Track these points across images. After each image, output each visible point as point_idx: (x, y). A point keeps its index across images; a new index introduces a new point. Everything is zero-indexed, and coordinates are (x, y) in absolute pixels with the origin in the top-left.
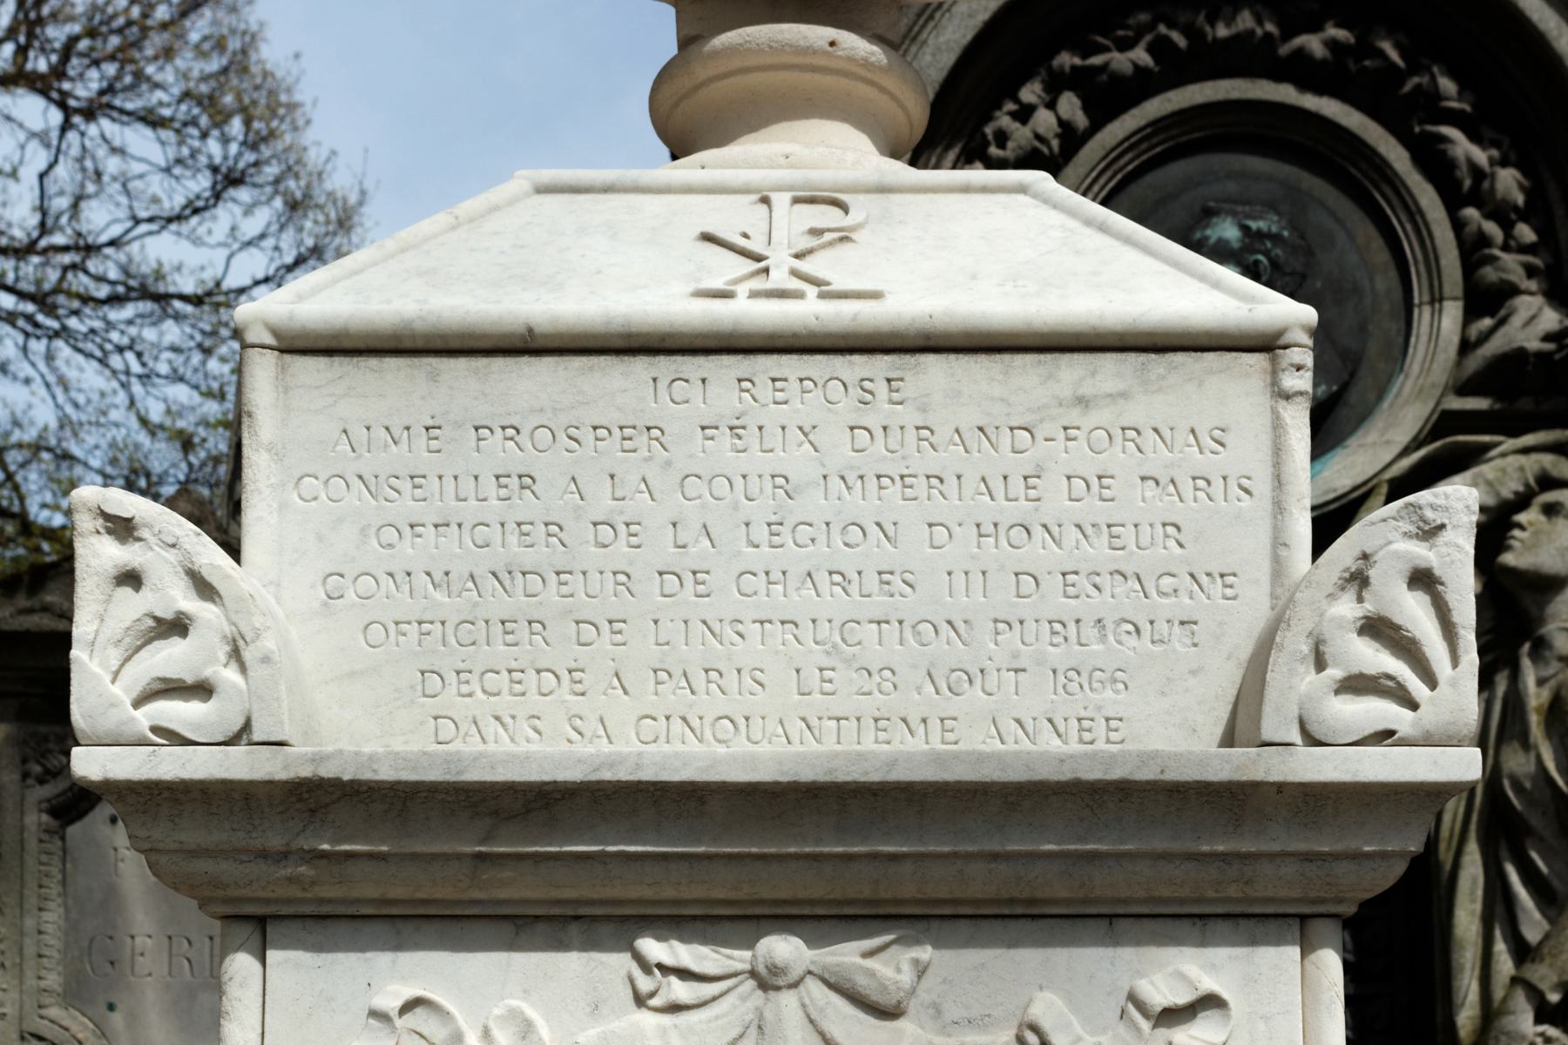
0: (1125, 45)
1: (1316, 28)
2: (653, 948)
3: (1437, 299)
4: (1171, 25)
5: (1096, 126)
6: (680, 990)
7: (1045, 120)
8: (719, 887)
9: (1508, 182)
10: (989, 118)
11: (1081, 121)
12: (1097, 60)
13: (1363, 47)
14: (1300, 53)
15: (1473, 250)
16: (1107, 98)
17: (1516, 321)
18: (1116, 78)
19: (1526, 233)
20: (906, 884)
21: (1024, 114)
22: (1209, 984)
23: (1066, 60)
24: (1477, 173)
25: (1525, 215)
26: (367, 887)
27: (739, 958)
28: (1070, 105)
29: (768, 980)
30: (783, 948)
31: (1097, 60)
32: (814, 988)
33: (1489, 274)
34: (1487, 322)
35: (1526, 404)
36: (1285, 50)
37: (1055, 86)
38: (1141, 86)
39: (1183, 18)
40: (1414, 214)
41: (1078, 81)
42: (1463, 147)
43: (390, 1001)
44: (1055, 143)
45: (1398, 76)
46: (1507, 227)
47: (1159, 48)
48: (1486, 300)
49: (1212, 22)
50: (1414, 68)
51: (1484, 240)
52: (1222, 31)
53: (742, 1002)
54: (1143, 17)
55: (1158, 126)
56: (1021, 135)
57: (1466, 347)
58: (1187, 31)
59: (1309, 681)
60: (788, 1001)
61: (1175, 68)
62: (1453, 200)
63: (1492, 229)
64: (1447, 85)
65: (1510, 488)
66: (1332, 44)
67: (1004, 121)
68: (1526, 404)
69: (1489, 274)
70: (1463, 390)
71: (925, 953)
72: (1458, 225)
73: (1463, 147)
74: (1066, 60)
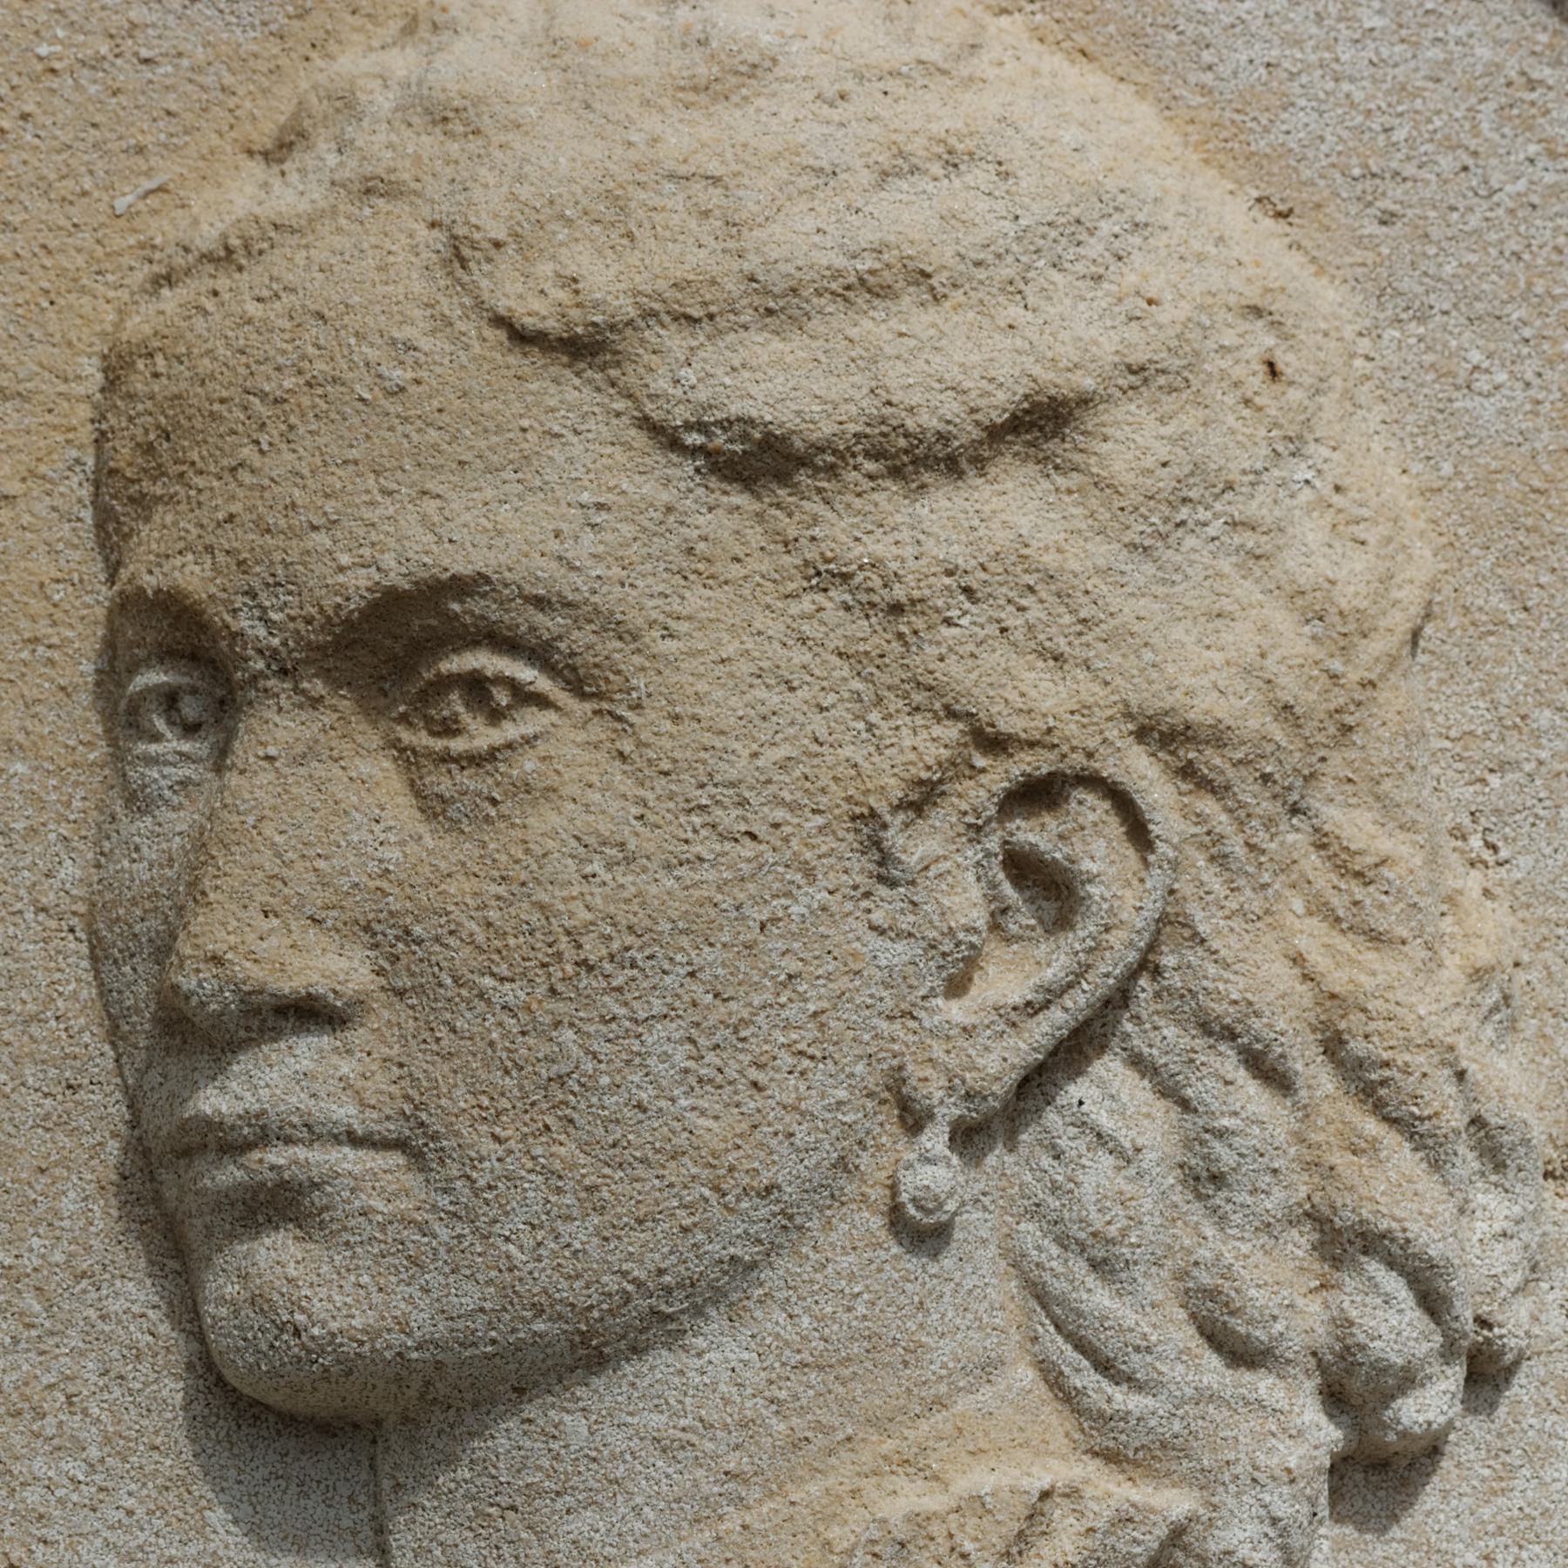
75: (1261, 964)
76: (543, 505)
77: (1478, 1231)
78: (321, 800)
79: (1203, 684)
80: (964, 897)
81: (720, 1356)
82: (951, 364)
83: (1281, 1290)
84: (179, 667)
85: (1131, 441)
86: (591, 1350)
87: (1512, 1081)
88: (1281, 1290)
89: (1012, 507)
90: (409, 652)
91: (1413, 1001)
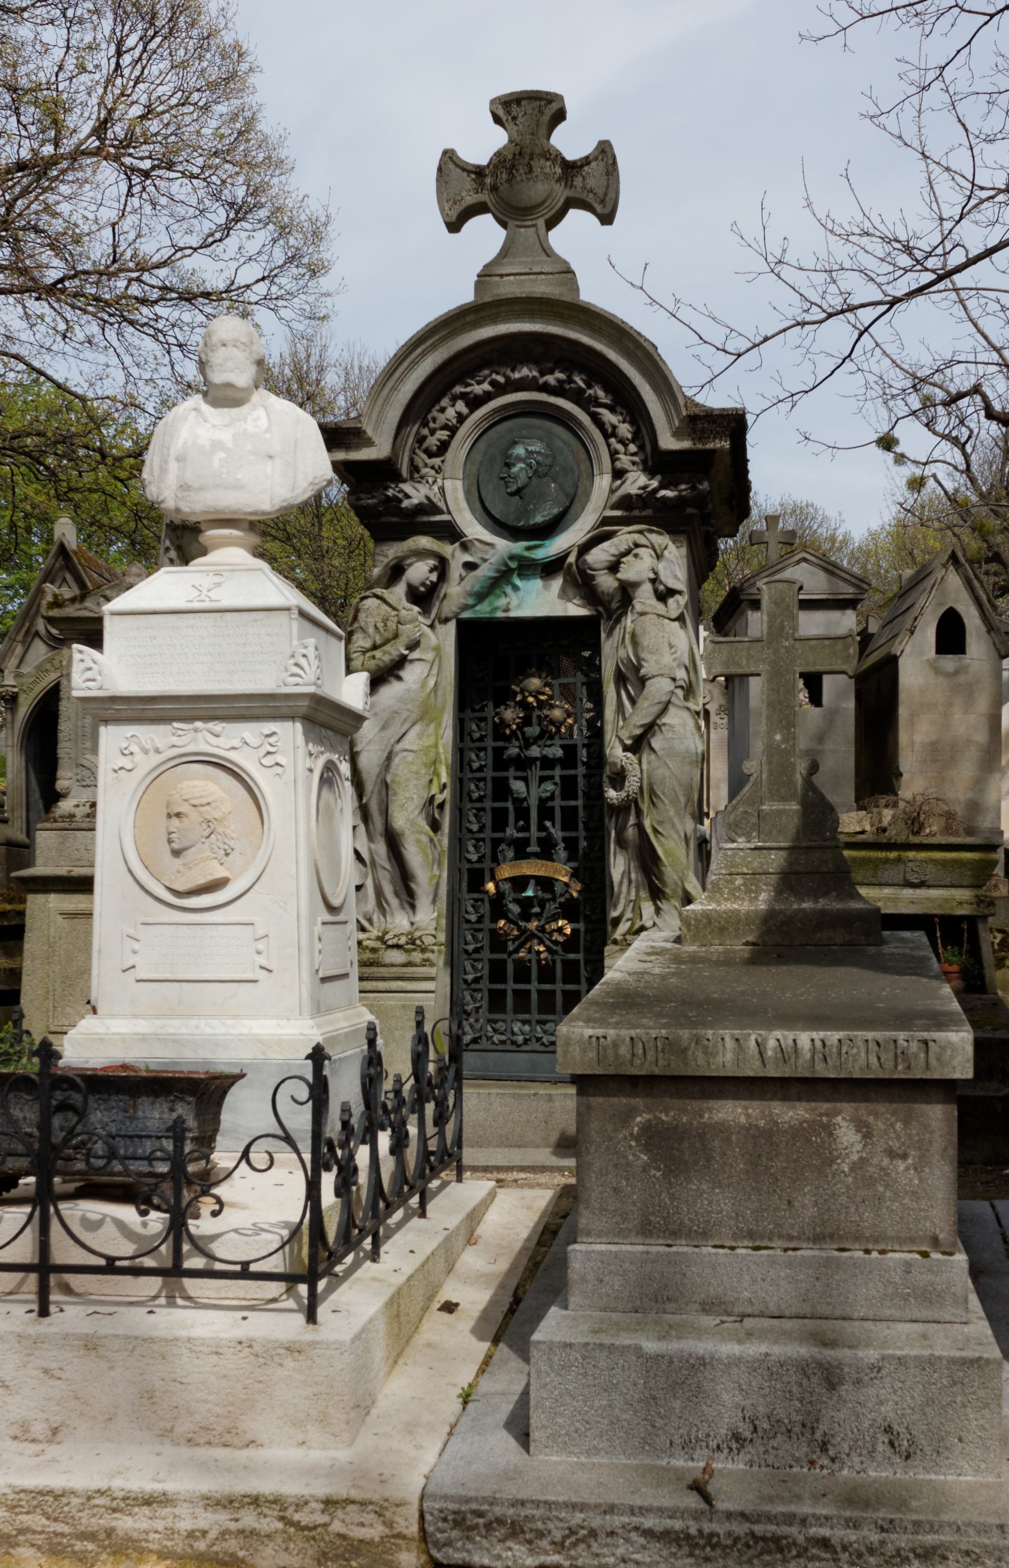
0: (479, 383)
1: (552, 372)
2: (175, 725)
3: (601, 473)
4: (498, 373)
5: (471, 412)
6: (180, 732)
7: (451, 413)
8: (186, 713)
9: (625, 430)
10: (429, 411)
11: (465, 410)
12: (469, 389)
13: (570, 380)
14: (546, 383)
15: (613, 454)
16: (474, 403)
17: (628, 482)
18: (476, 396)
19: (633, 448)
20: (219, 713)
21: (443, 410)
22: (274, 729)
23: (459, 389)
24: (614, 427)
25: (633, 441)
26: (124, 715)
27: (190, 726)
28: (461, 406)
29: (196, 730)
30: (198, 724)
31: (469, 389)
32: (205, 733)
33: (618, 464)
34: (619, 482)
35: (636, 513)
36: (541, 381)
37: (454, 399)
38: (487, 397)
39: (502, 371)
40: (593, 441)
41: (463, 396)
42: (609, 417)
43: (129, 735)
44: (454, 421)
45: (584, 391)
46: (625, 445)
47: (493, 383)
48: (618, 474)
49: (513, 370)
50: (590, 387)
51: (617, 452)
52: (517, 375)
53: (192, 734)
54: (486, 372)
55: (496, 411)
56: (442, 419)
57: (612, 491)
58: (504, 375)
59: (285, 675)
60: (199, 734)
61: (500, 389)
62: (606, 436)
63: (620, 447)
64: (601, 393)
65: (623, 548)
66: (558, 380)
67: (434, 413)
68: (636, 513)
69: (618, 464)
70: (613, 508)
71: (224, 725)
72: (609, 445)
73: (609, 417)
74: (459, 389)
75: (220, 830)
76: (184, 808)
77: (232, 843)
78: (175, 821)
79: (216, 816)
80: (205, 826)
81: (194, 849)
82: (204, 801)
83: (221, 846)
84: (169, 816)
85: (213, 805)
86: (186, 849)
87: (234, 835)
88: (221, 846)
89: (207, 808)
90: (178, 815)
91: (228, 832)
